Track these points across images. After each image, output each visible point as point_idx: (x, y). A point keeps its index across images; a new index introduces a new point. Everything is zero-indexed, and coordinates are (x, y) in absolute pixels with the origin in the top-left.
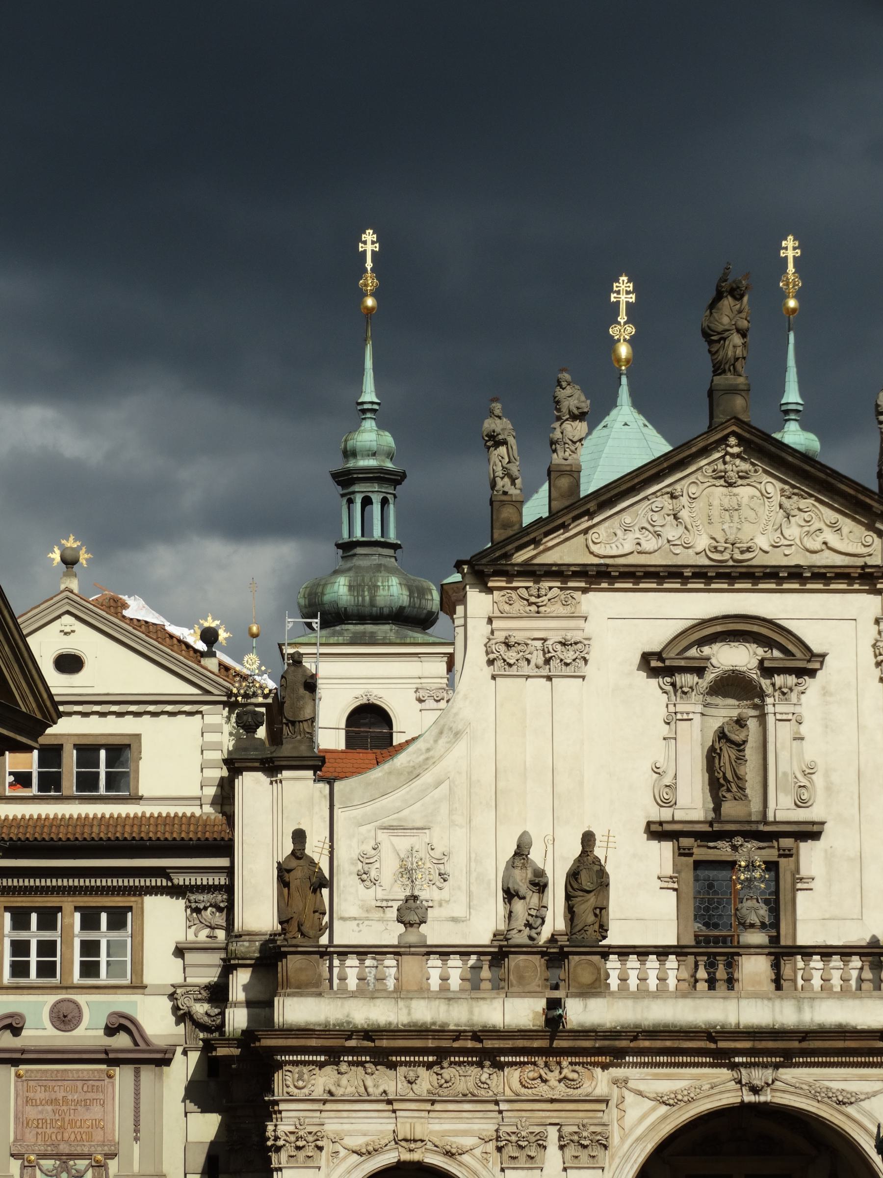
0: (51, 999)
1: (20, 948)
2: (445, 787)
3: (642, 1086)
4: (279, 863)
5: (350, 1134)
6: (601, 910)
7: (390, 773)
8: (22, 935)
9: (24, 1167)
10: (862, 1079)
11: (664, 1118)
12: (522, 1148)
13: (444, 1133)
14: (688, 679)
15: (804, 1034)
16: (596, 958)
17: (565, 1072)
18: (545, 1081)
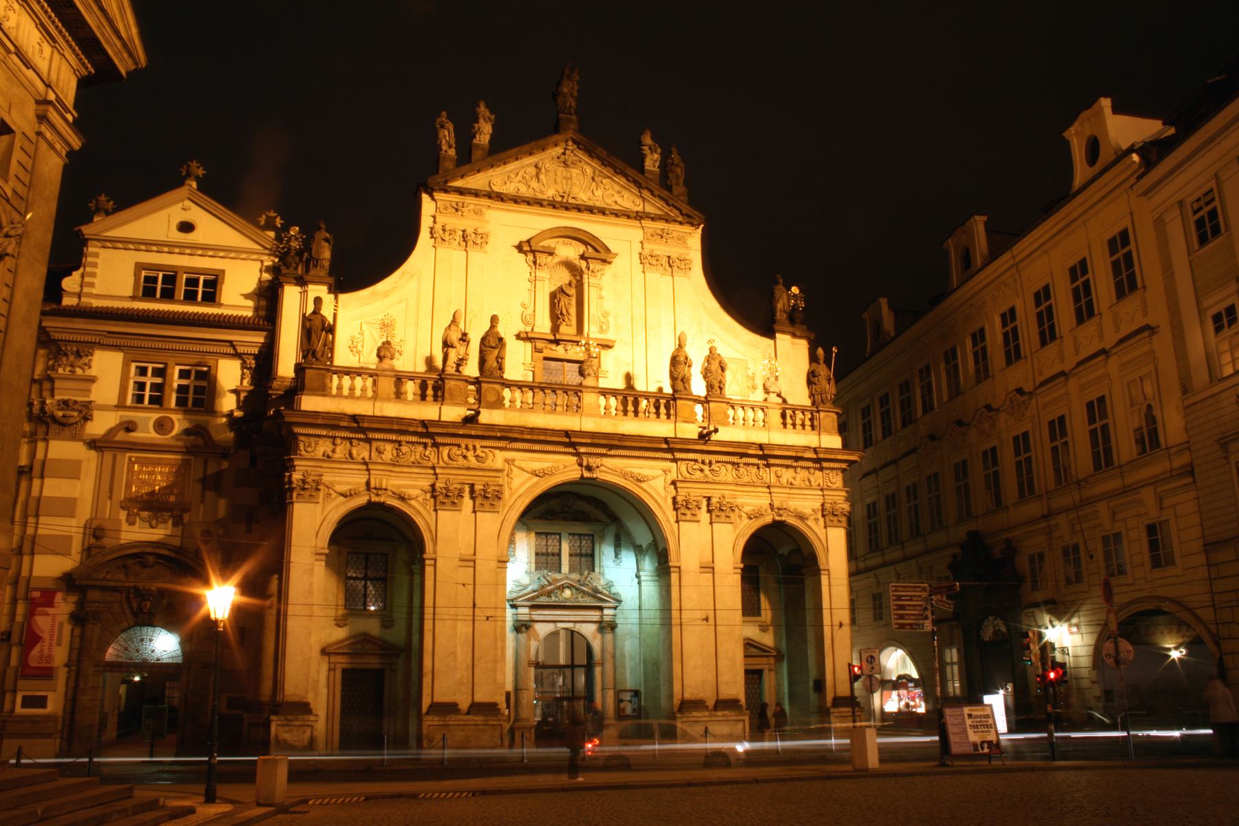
0: (155, 416)
1: (141, 386)
2: (404, 303)
3: (523, 465)
4: (304, 315)
5: (339, 483)
6: (500, 360)
7: (373, 293)
8: (142, 379)
9: (128, 515)
10: (651, 468)
11: (536, 484)
12: (447, 496)
13: (399, 486)
14: (542, 259)
15: (623, 437)
16: (497, 387)
17: (479, 452)
18: (465, 457)
